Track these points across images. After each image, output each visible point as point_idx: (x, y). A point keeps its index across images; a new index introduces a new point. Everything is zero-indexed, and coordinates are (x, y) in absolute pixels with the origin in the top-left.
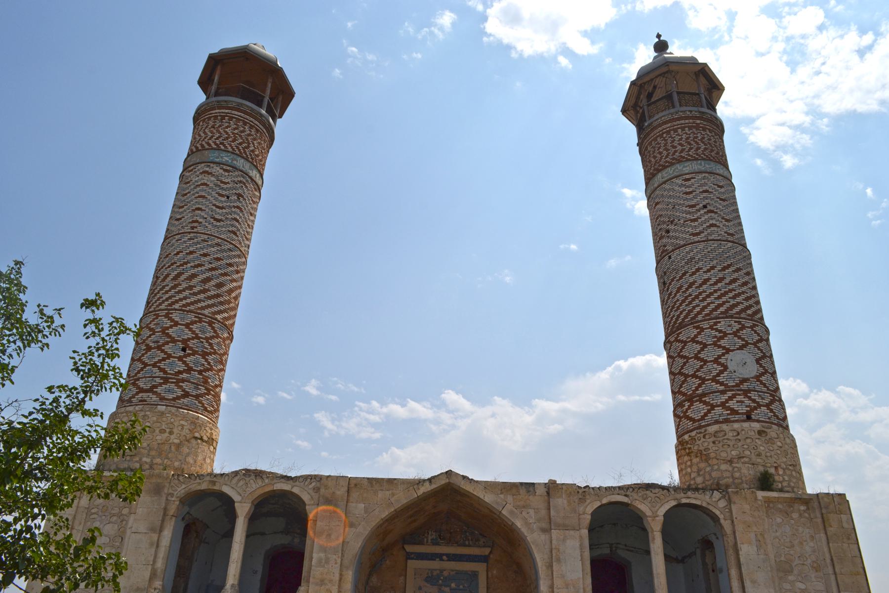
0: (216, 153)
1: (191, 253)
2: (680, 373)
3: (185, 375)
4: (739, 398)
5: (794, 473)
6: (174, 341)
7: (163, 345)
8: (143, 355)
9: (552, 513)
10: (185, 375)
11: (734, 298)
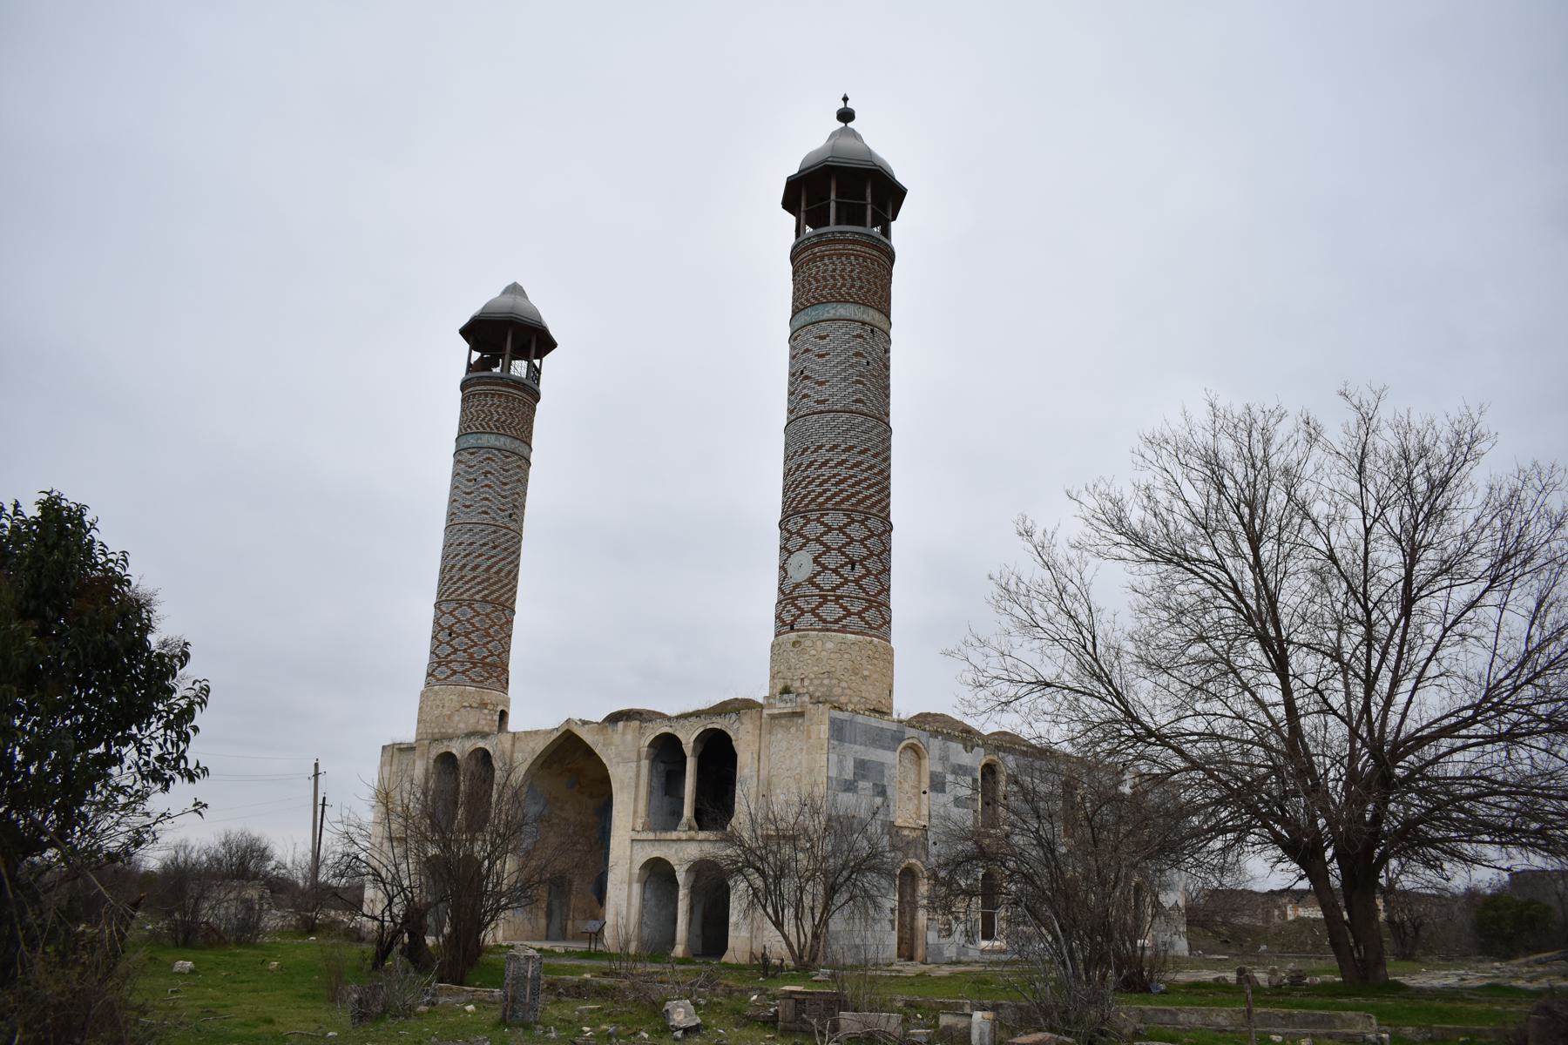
5: (826, 682)
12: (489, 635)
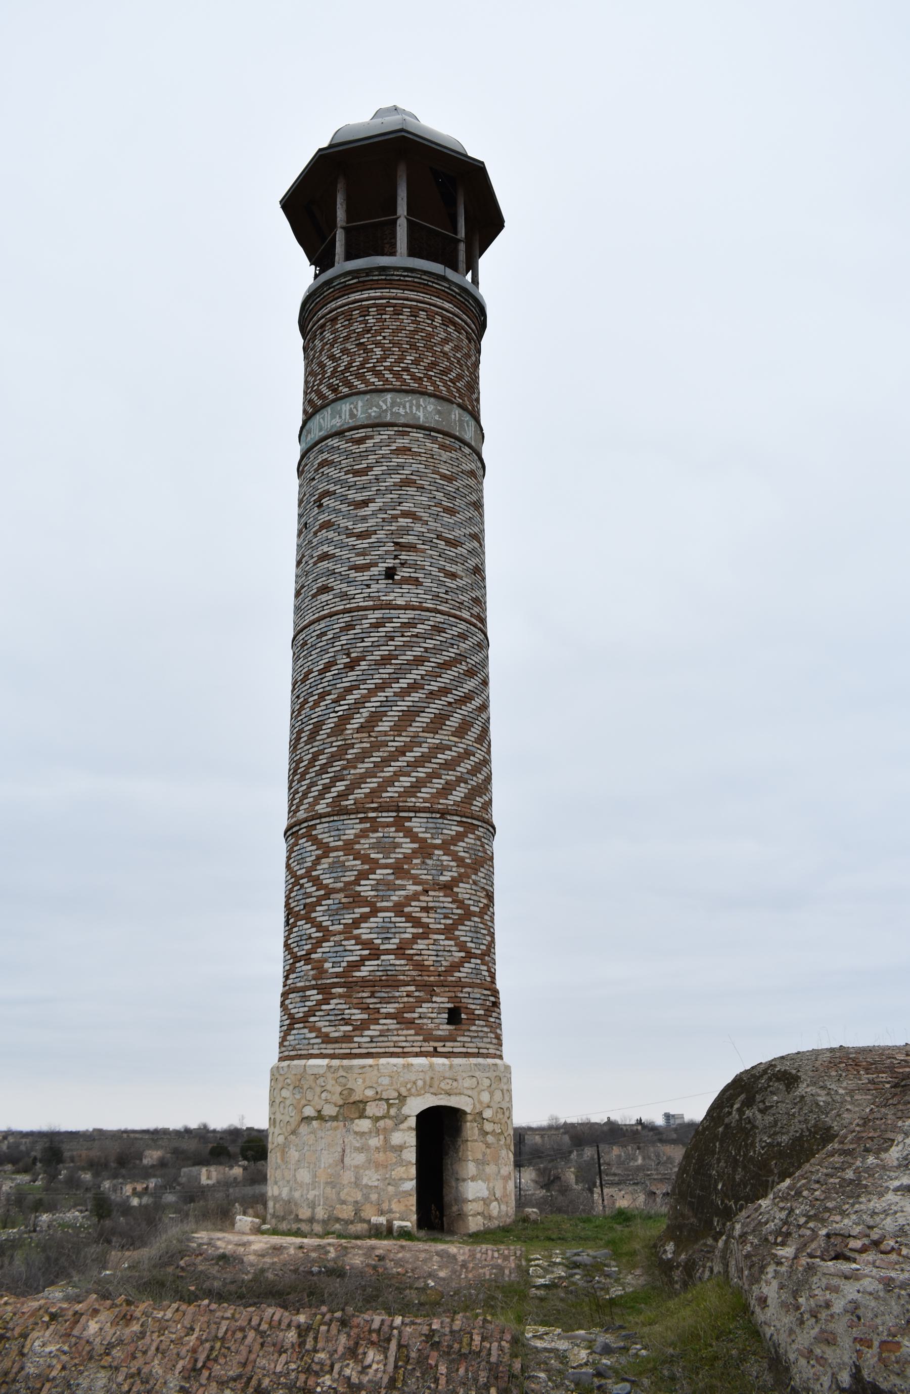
12: (357, 900)
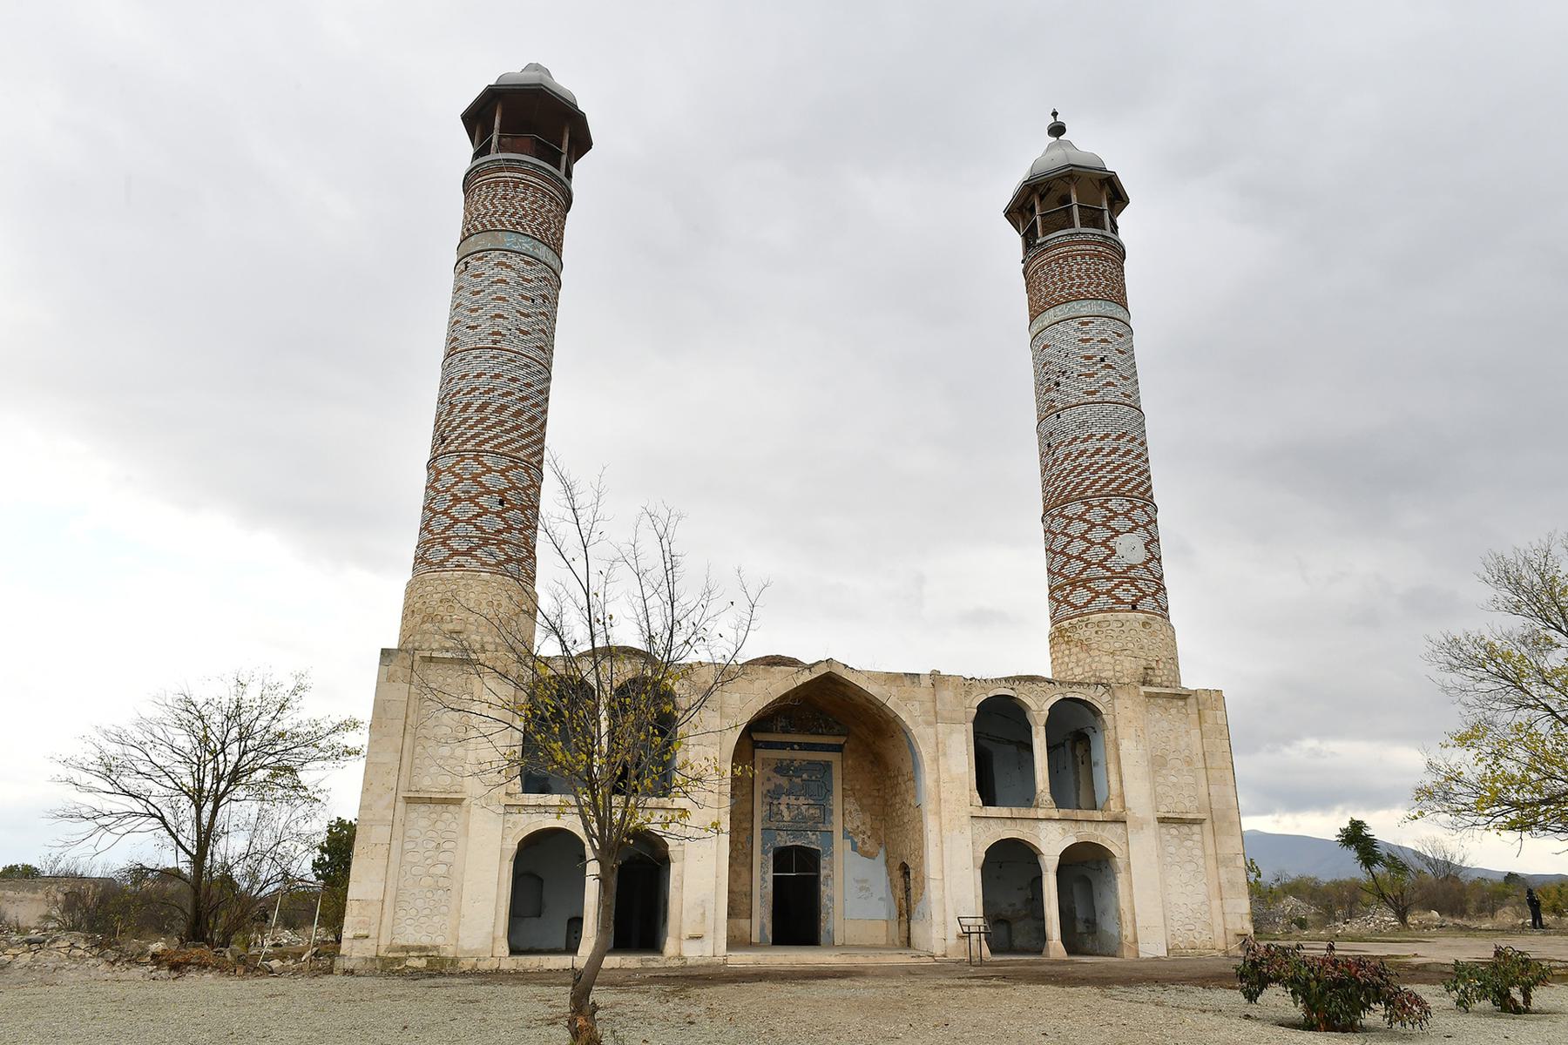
0: (514, 237)
1: (497, 376)
2: (1062, 552)
3: (505, 535)
4: (1126, 586)
6: (489, 492)
7: (477, 496)
8: (450, 507)
9: (939, 706)
10: (505, 535)
11: (1127, 472)
